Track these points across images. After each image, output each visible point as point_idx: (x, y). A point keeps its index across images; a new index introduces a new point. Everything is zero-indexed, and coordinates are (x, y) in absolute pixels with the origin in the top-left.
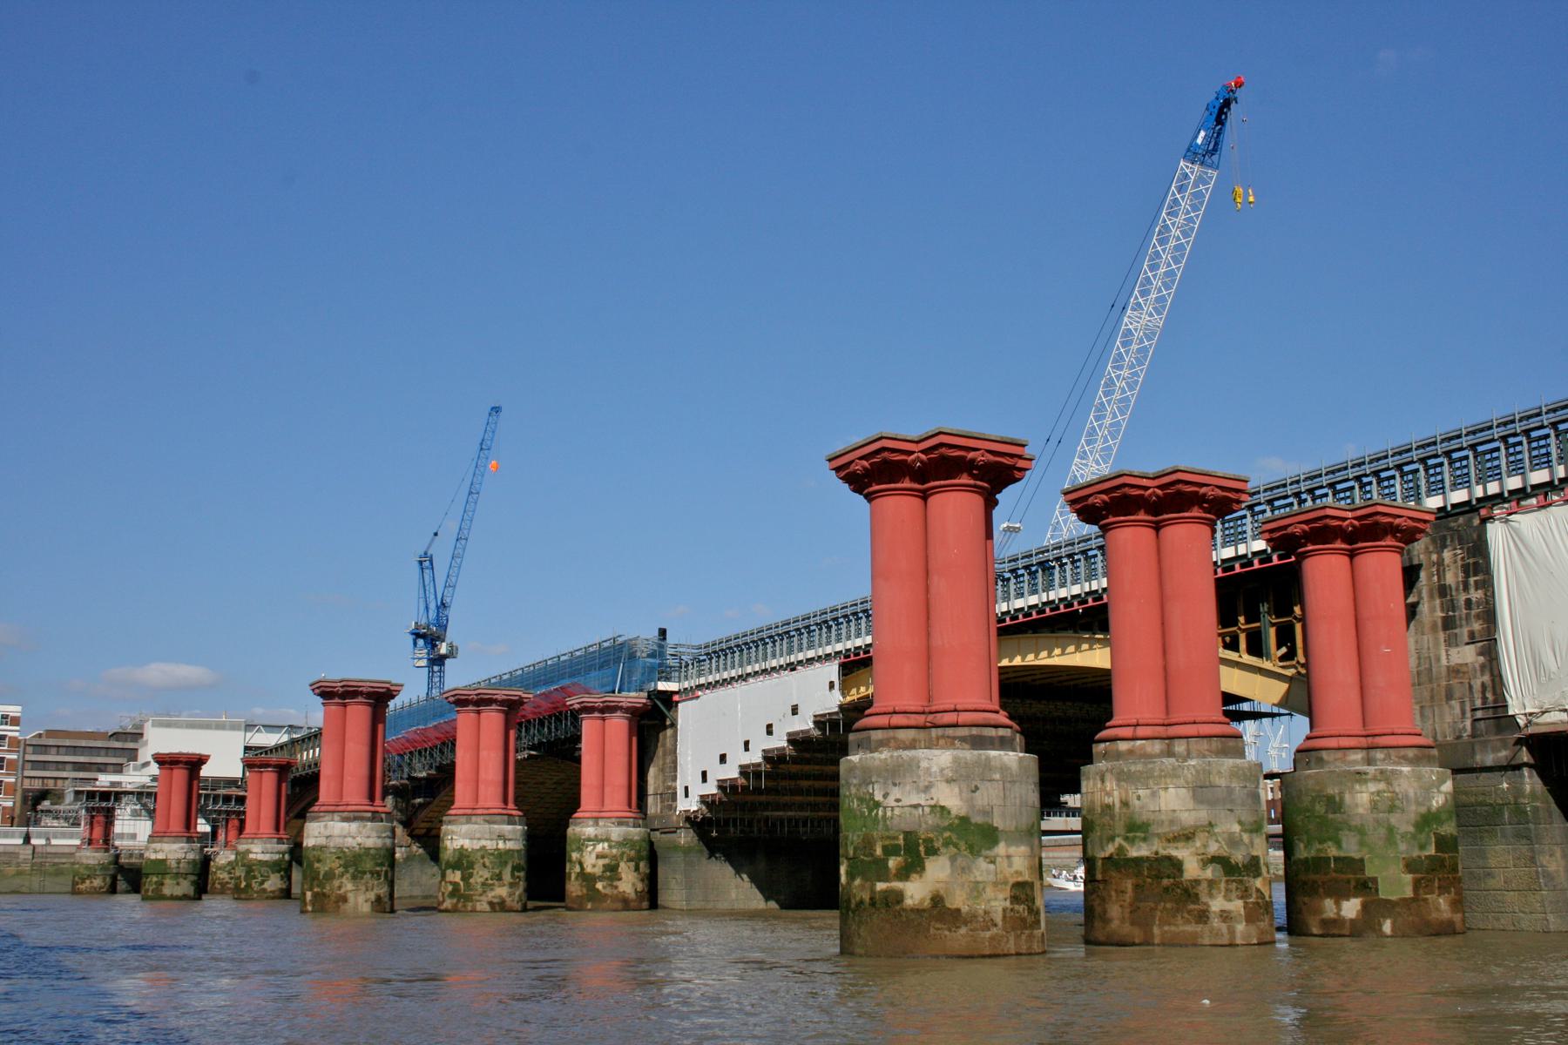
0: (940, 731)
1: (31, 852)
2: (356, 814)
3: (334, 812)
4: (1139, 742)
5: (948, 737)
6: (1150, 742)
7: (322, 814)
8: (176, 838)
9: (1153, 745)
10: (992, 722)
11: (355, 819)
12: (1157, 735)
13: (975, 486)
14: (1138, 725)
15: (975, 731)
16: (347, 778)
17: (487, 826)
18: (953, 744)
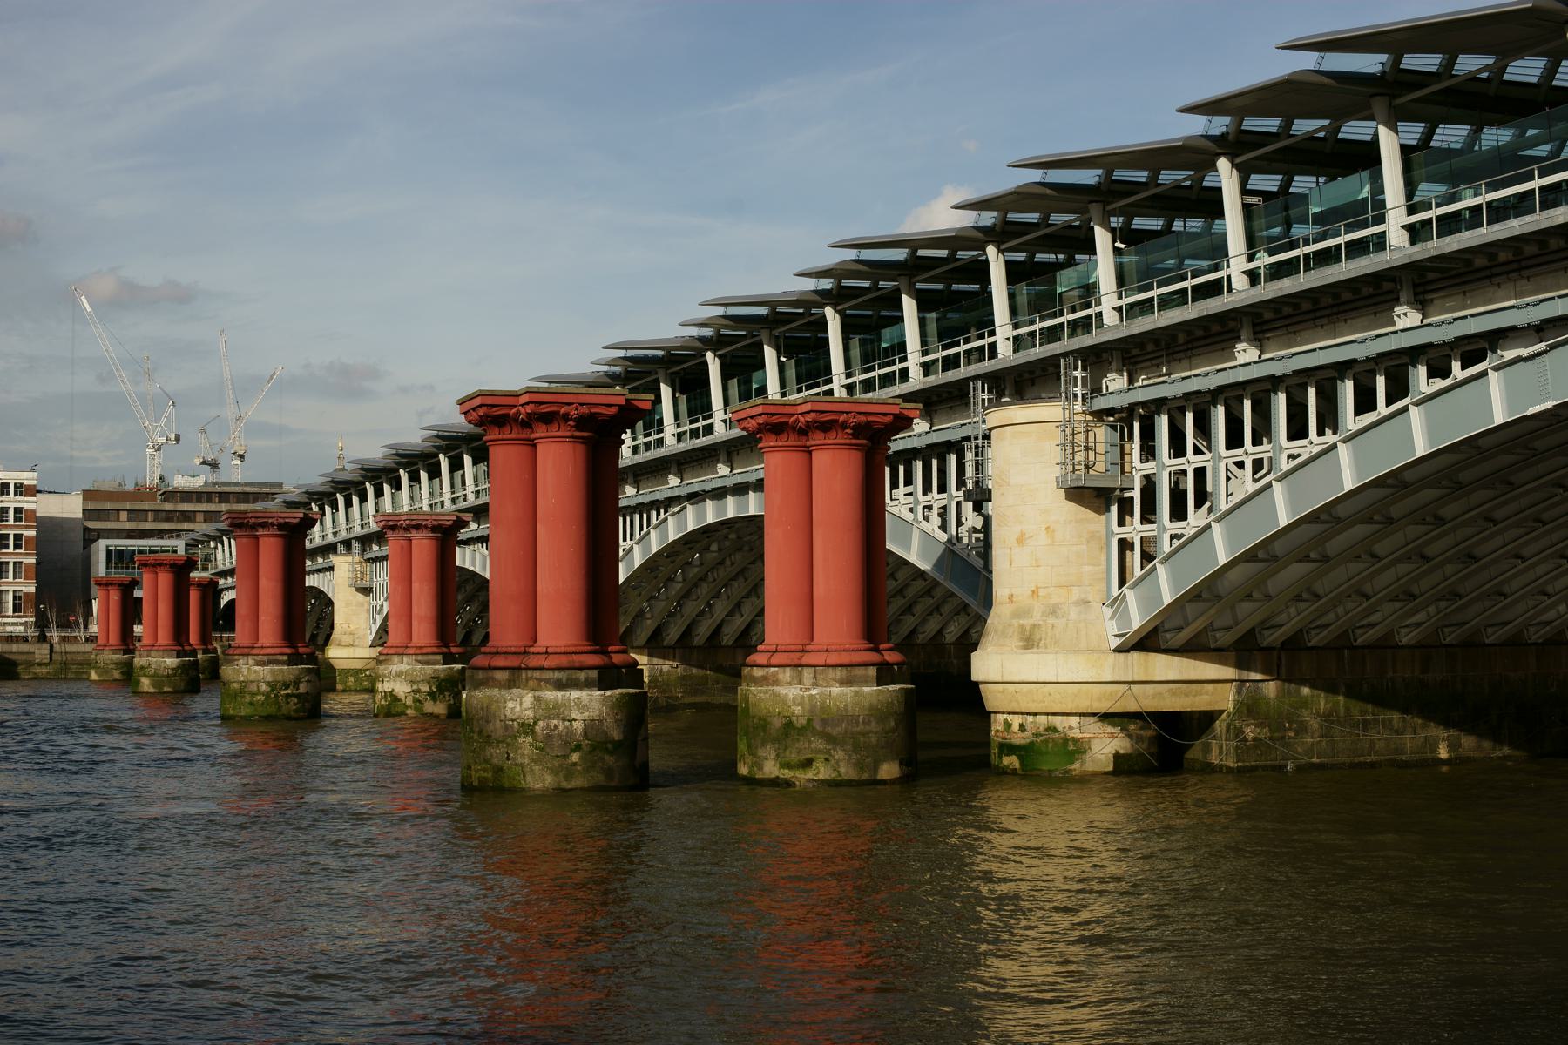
0: (530, 673)
1: (47, 651)
2: (271, 658)
3: (248, 655)
4: (772, 669)
5: (536, 679)
6: (782, 669)
7: (236, 657)
8: (166, 651)
9: (784, 672)
10: (577, 665)
11: (270, 662)
12: (789, 662)
13: (572, 437)
14: (776, 651)
15: (557, 675)
16: (262, 618)
17: (419, 666)
18: (539, 685)
